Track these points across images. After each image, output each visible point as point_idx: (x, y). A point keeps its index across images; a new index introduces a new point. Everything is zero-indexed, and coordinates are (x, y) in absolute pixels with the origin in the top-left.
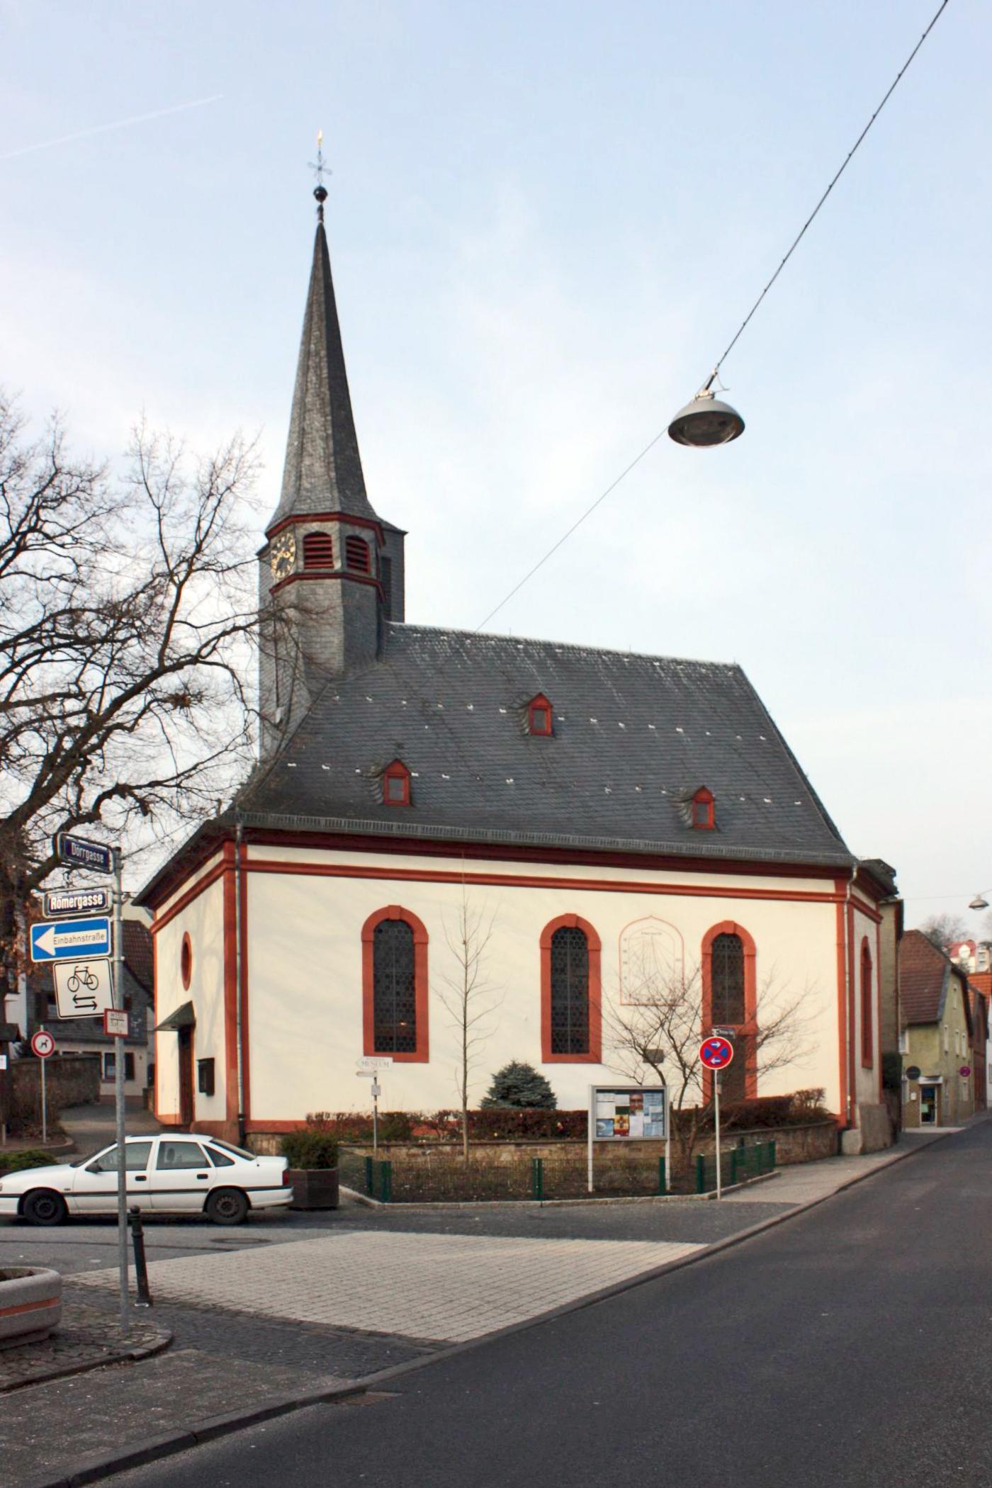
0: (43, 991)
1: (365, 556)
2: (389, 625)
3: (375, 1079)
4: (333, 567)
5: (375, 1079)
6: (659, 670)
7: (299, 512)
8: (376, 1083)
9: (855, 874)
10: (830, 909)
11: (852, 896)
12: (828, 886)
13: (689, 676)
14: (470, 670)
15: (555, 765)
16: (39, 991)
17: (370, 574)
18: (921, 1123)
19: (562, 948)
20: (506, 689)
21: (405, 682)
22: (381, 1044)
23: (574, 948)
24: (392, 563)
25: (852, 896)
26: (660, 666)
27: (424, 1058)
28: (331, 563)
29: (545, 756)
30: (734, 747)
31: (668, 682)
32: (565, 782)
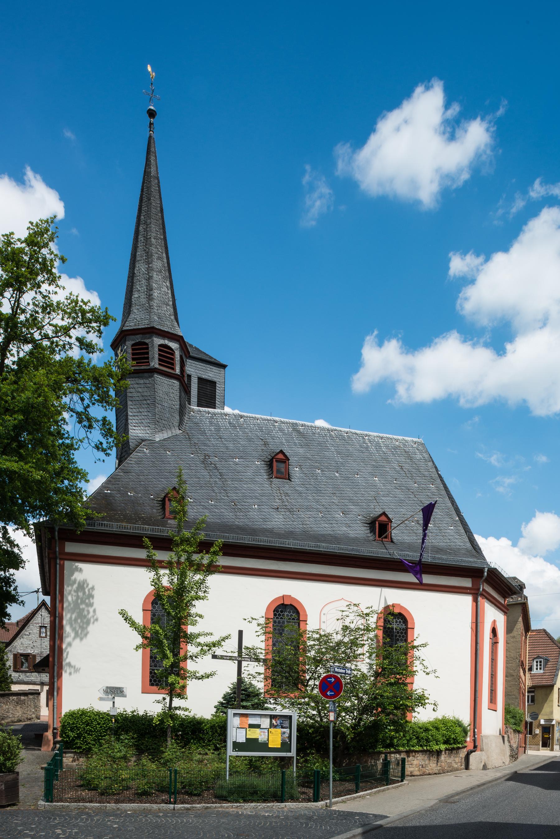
0: (18, 653)
1: (173, 359)
2: (190, 408)
3: (114, 702)
4: (149, 365)
5: (114, 702)
6: (367, 441)
7: (128, 328)
8: (114, 706)
9: (486, 574)
10: (468, 600)
11: (483, 590)
12: (467, 583)
13: (387, 446)
14: (241, 437)
15: (287, 498)
16: (15, 653)
17: (173, 369)
18: (541, 748)
19: (281, 618)
20: (263, 450)
21: (195, 443)
22: (155, 681)
23: (277, 618)
24: (217, 385)
25: (483, 590)
26: (368, 439)
27: (144, 691)
28: (148, 362)
29: (282, 492)
30: (412, 491)
31: (373, 449)
32: (293, 509)
